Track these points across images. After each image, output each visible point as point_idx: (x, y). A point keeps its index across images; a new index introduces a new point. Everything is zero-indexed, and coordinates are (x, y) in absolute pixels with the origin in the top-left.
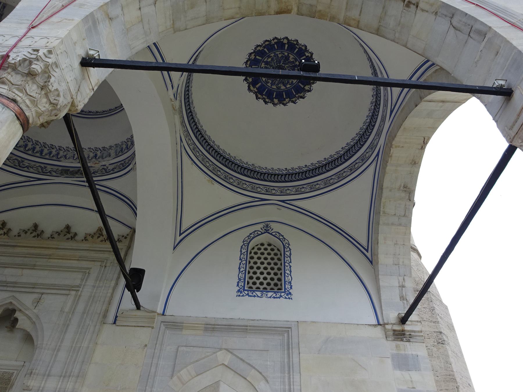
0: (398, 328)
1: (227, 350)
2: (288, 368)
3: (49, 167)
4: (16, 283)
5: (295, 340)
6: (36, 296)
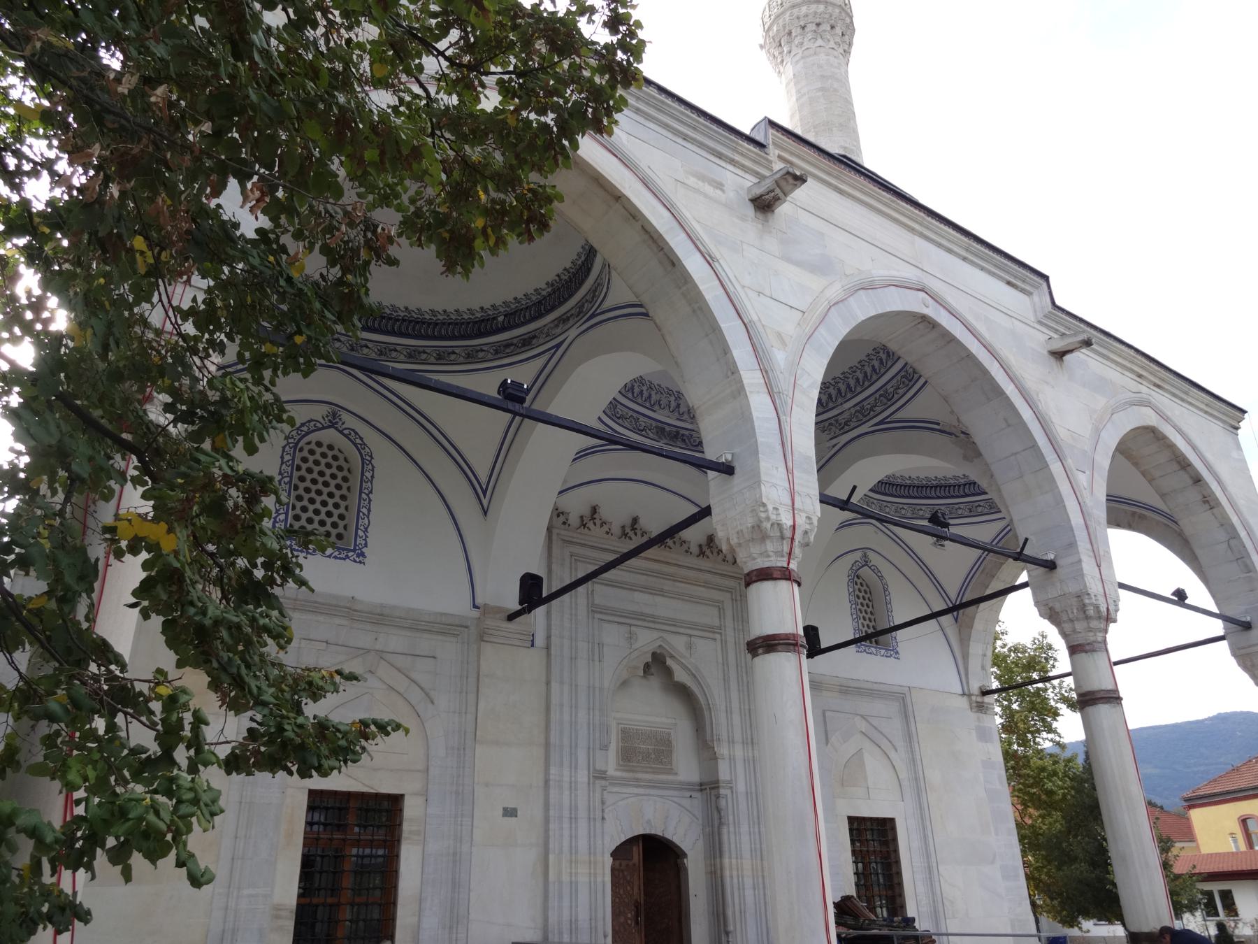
0: (979, 699)
1: (862, 716)
2: (909, 738)
3: (642, 418)
4: (653, 616)
5: (910, 708)
6: (685, 639)
